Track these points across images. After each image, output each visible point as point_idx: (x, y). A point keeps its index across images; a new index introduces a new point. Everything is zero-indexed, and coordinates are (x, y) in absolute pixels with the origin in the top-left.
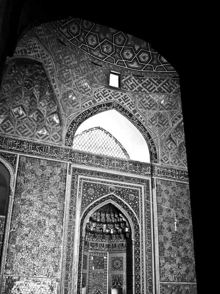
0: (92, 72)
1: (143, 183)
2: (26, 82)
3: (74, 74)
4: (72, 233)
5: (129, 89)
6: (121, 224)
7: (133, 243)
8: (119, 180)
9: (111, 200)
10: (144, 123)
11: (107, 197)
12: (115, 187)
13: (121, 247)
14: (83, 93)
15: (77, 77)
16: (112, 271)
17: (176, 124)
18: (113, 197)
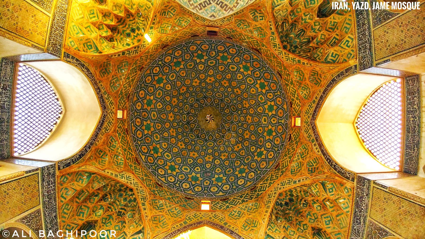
0: (185, 203)
2: (121, 210)
3: (167, 204)
5: (218, 209)
10: (237, 232)
14: (175, 217)
15: (170, 206)
17: (266, 219)
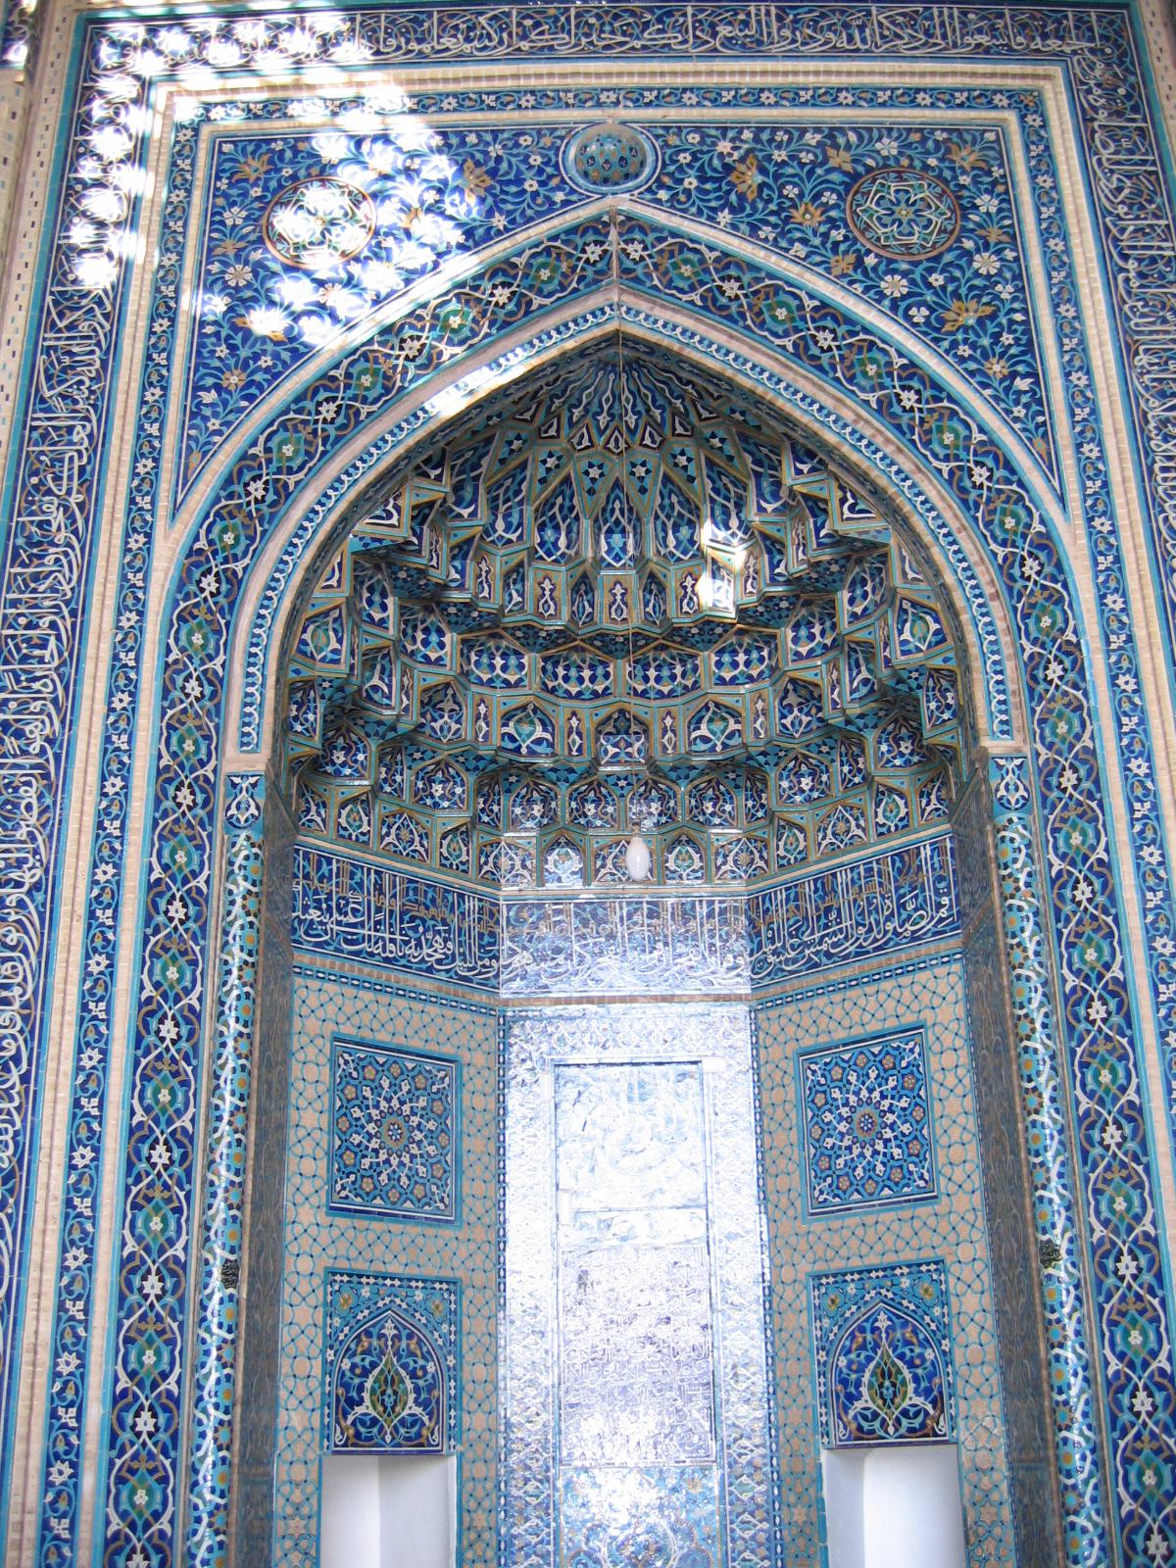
1: (1053, 44)
4: (37, 732)
6: (845, 595)
7: (1008, 786)
8: (699, 42)
9: (630, 300)
11: (546, 251)
12: (650, 126)
13: (891, 904)
16: (818, 1226)
18: (635, 250)
